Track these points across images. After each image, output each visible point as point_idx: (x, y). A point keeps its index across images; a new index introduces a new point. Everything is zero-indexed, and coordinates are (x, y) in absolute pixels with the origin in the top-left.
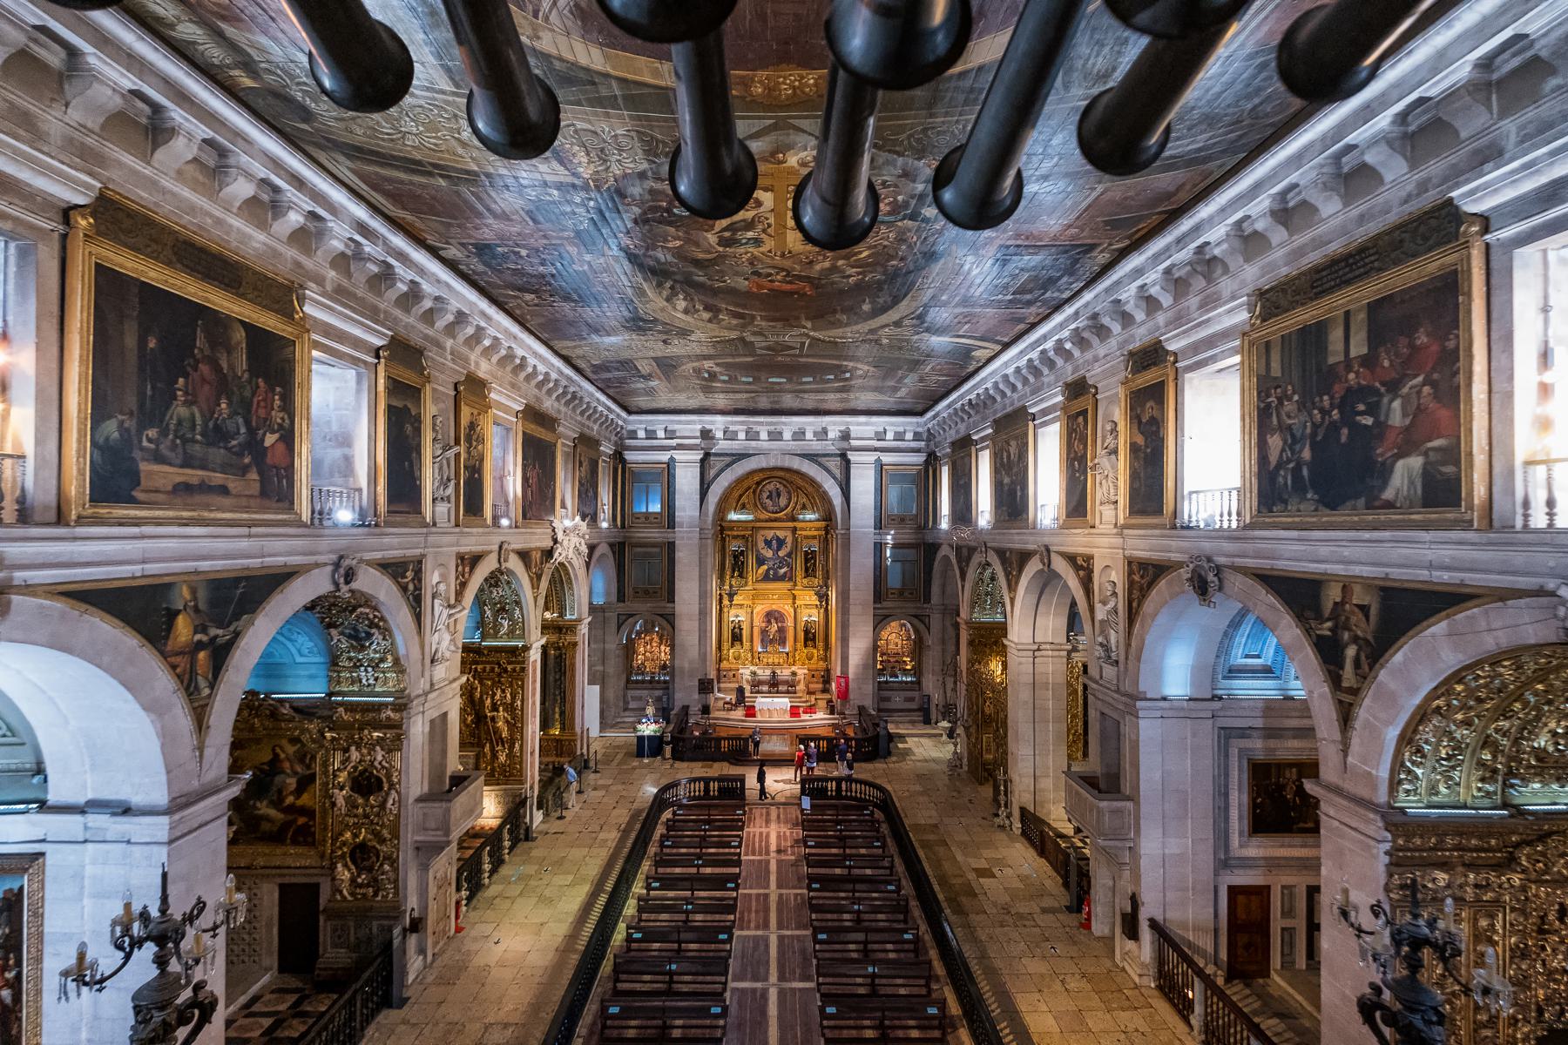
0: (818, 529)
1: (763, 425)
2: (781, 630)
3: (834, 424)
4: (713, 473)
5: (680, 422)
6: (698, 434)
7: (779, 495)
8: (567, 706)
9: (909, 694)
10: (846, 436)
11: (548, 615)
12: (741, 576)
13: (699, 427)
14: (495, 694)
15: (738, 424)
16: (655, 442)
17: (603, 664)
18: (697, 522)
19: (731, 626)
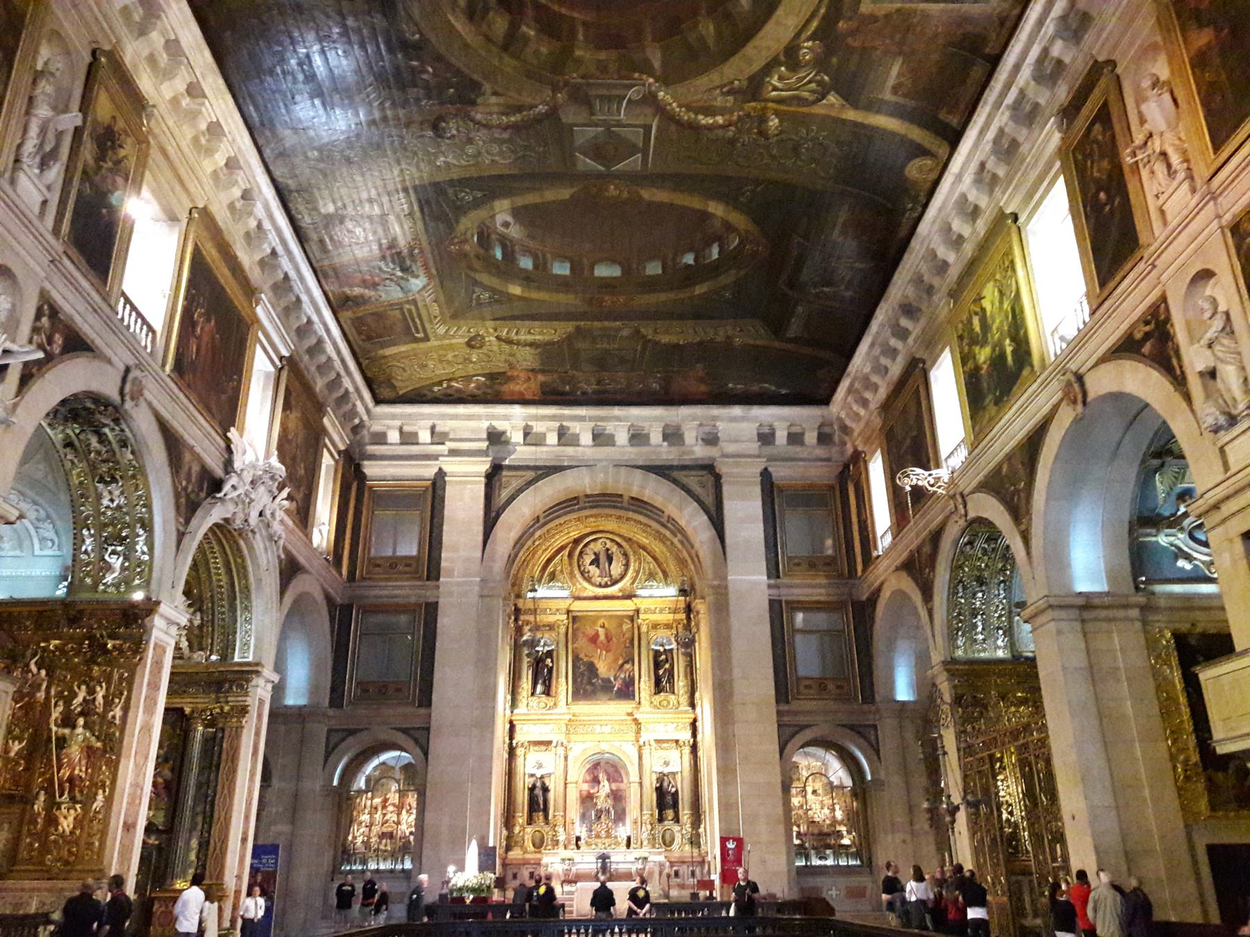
0: (675, 611)
1: (581, 420)
2: (617, 797)
4: (505, 494)
6: (484, 436)
7: (610, 559)
8: (215, 829)
9: (855, 881)
11: (199, 656)
12: (547, 692)
13: (485, 424)
14: (76, 695)
15: (545, 418)
16: (414, 449)
18: (475, 566)
19: (529, 782)
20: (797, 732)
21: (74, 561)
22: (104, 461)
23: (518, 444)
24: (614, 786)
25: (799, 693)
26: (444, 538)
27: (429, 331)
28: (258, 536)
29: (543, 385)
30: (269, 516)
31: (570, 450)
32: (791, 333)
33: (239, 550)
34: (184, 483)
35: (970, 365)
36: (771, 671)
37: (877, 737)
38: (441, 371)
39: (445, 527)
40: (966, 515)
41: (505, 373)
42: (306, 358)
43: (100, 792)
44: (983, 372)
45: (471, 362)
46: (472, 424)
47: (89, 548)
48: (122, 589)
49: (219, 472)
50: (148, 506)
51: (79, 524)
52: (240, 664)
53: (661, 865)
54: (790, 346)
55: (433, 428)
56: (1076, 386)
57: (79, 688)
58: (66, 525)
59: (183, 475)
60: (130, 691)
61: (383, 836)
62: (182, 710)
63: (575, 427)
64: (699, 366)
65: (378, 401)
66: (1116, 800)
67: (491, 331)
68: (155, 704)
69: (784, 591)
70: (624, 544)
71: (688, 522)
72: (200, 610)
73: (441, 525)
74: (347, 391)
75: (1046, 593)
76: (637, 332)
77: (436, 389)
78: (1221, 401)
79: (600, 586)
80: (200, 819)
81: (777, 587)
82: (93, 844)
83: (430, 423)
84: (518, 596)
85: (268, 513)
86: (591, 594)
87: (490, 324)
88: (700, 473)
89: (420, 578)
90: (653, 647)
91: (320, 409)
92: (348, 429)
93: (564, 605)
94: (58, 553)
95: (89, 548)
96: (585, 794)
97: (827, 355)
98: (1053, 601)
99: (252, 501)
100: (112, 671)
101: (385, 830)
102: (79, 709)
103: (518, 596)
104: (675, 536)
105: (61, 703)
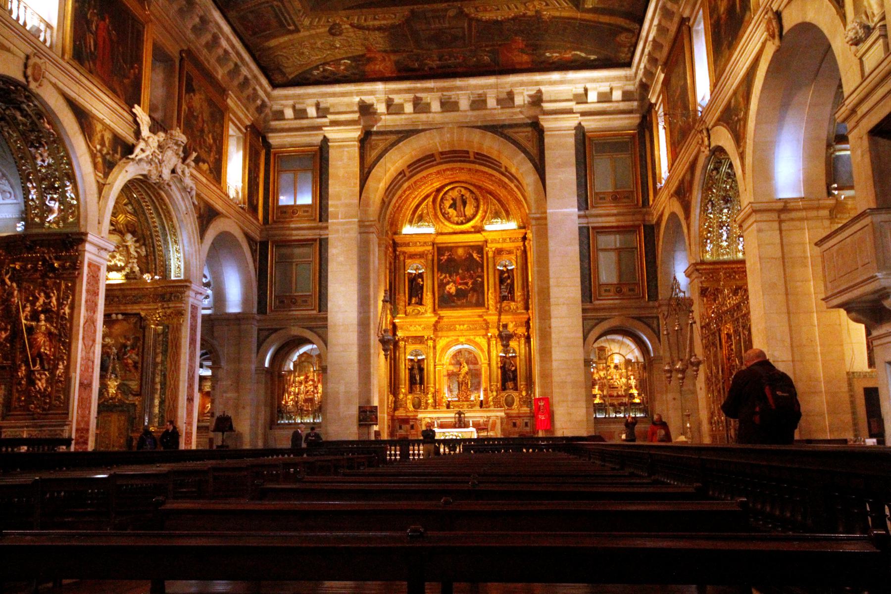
0: (513, 240)
2: (475, 374)
3: (522, 84)
4: (374, 154)
5: (334, 95)
6: (356, 108)
7: (464, 203)
10: (537, 100)
11: (147, 277)
13: (357, 99)
14: (37, 299)
16: (305, 122)
17: (237, 390)
18: (355, 210)
20: (596, 324)
21: (26, 206)
22: (32, 131)
23: (383, 114)
24: (471, 366)
25: (600, 295)
26: (331, 190)
27: (296, 23)
28: (173, 187)
29: (397, 63)
30: (180, 173)
31: (423, 117)
32: (589, 5)
33: (162, 199)
34: (98, 147)
35: (715, 16)
36: (579, 280)
37: (658, 325)
38: (316, 57)
39: (330, 182)
40: (709, 146)
41: (363, 56)
42: (205, 51)
43: (61, 363)
44: (722, 22)
45: (336, 48)
46: (346, 100)
47: (35, 197)
48: (61, 224)
49: (131, 139)
50: (70, 163)
51: (25, 178)
52: (174, 281)
53: (502, 418)
54: (588, 16)
55: (317, 105)
56: (774, 23)
57: (39, 295)
58: (16, 181)
59: (97, 141)
60: (74, 295)
61: (306, 401)
62: (139, 314)
63: (426, 97)
64: (519, 39)
65: (275, 85)
66: (793, 355)
67: (345, 19)
68: (96, 305)
69: (591, 220)
70: (475, 190)
71: (517, 169)
72: (144, 244)
73: (327, 180)
74: (246, 78)
75: (752, 200)
76: (461, 12)
77: (315, 72)
78: (864, 17)
79: (457, 224)
80: (159, 387)
81: (586, 216)
82: (59, 397)
83: (314, 101)
84: (395, 233)
85: (179, 171)
86: (451, 230)
87: (342, 13)
88: (525, 130)
89: (315, 220)
90: (498, 267)
91: (223, 92)
92: (252, 108)
93: (429, 239)
94: (15, 201)
95: (35, 197)
96: (450, 372)
97: (620, 21)
98: (757, 206)
99: (161, 162)
100: (60, 283)
101: (306, 397)
102: (40, 309)
103: (395, 233)
104: (512, 181)
105: (28, 305)
